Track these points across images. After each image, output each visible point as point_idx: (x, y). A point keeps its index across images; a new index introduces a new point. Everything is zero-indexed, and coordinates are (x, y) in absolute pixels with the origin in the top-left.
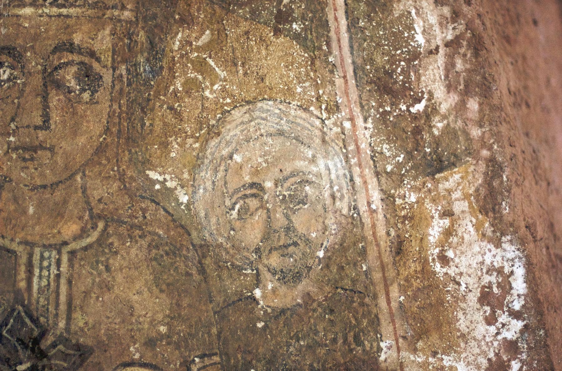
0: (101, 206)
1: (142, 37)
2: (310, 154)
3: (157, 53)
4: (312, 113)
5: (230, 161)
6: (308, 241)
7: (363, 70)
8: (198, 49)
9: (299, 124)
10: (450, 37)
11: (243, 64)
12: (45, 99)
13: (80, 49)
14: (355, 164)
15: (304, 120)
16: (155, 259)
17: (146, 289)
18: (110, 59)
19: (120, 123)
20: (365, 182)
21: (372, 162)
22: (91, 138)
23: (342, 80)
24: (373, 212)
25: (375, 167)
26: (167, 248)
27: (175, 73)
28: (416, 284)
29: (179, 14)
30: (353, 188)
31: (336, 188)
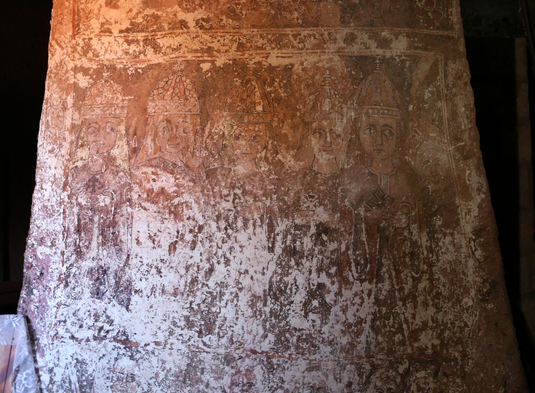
1: (402, 124)
2: (440, 154)
6: (439, 174)
8: (415, 127)
12: (382, 138)
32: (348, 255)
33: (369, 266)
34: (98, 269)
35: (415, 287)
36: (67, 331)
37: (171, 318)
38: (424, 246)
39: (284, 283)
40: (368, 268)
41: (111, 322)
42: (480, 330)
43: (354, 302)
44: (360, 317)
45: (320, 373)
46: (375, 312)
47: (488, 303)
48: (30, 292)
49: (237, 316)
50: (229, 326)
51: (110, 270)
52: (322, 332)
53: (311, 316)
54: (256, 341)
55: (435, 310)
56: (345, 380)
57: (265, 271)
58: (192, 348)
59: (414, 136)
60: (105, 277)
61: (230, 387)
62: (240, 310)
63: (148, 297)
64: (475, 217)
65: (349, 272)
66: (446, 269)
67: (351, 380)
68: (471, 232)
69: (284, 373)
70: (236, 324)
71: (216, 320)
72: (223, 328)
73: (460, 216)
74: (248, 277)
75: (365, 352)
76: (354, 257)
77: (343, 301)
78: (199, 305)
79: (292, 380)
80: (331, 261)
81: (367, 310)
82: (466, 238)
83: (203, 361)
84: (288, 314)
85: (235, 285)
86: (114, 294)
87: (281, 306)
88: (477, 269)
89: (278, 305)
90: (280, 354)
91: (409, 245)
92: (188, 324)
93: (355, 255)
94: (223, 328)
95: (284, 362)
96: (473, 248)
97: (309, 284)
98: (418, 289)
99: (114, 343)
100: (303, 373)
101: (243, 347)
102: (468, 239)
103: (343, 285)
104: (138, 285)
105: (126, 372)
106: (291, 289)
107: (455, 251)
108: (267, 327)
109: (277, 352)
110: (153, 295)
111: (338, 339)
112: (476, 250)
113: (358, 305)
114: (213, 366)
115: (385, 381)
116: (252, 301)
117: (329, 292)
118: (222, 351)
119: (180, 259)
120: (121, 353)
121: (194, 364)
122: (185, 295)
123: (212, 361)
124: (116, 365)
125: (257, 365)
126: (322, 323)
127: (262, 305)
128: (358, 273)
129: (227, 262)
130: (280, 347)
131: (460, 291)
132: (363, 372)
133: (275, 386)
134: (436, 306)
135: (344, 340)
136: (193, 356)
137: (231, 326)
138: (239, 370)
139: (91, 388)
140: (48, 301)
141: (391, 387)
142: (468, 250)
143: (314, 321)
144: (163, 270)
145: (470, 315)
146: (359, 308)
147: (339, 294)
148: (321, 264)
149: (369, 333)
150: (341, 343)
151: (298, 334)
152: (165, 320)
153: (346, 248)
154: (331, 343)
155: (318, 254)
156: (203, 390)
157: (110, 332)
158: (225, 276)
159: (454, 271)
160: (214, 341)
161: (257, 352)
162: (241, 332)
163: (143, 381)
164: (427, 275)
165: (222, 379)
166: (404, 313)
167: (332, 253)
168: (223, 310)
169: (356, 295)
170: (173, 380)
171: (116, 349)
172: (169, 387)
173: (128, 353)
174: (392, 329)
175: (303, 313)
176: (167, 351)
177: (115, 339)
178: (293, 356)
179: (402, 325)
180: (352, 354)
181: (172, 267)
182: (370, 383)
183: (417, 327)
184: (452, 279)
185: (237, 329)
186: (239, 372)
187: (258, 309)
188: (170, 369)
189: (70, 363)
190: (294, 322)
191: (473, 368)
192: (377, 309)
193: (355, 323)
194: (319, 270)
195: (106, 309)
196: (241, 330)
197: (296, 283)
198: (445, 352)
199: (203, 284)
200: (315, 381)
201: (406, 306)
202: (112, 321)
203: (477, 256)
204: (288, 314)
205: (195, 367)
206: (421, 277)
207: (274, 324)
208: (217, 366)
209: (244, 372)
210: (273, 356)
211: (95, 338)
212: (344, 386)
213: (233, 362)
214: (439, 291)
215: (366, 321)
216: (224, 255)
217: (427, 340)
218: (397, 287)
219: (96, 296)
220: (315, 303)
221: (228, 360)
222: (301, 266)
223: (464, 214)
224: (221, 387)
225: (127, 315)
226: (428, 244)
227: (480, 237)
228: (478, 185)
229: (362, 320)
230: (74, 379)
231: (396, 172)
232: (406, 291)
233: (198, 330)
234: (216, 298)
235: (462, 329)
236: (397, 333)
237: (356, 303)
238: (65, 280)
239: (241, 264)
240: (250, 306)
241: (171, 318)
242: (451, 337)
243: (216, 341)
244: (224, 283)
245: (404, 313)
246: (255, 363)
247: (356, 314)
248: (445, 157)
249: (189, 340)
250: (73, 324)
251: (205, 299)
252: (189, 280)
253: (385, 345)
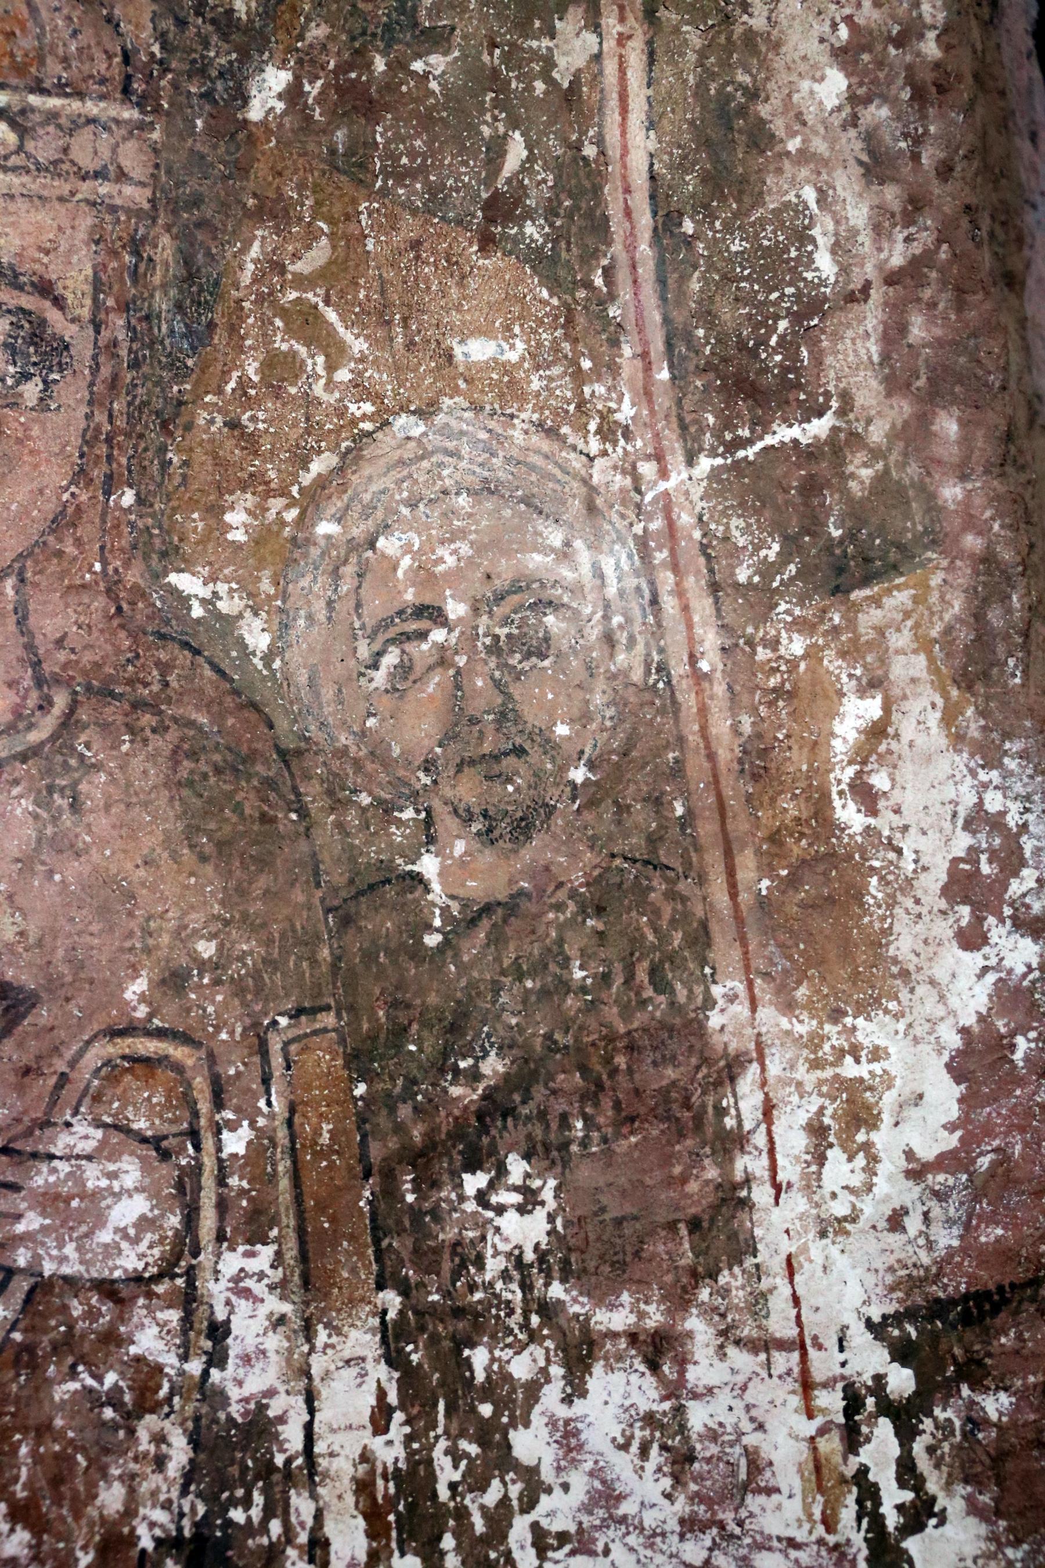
0: (62, 656)
1: (165, 249)
2: (556, 538)
3: (201, 291)
4: (562, 439)
5: (369, 553)
6: (550, 745)
7: (688, 337)
8: (301, 282)
9: (533, 468)
10: (897, 260)
11: (405, 320)
13: (16, 276)
14: (663, 563)
15: (547, 457)
16: (190, 784)
17: (165, 855)
18: (88, 302)
19: (110, 458)
20: (686, 609)
21: (702, 560)
22: (41, 492)
23: (639, 363)
24: (699, 678)
25: (711, 571)
26: (217, 757)
27: (243, 338)
28: (798, 848)
29: (255, 195)
30: (659, 624)
31: (617, 620)
38: (341, 1466)
59: (280, 369)
64: (917, 1171)
73: (749, 1163)
82: (807, 1385)
96: (893, 1497)
102: (832, 1401)
107: (689, 1526)
112: (920, 1514)
142: (830, 1523)
223: (792, 1142)
226: (390, 1451)
227: (975, 1373)
228: (962, 842)
231: (68, 722)
248: (617, 563)
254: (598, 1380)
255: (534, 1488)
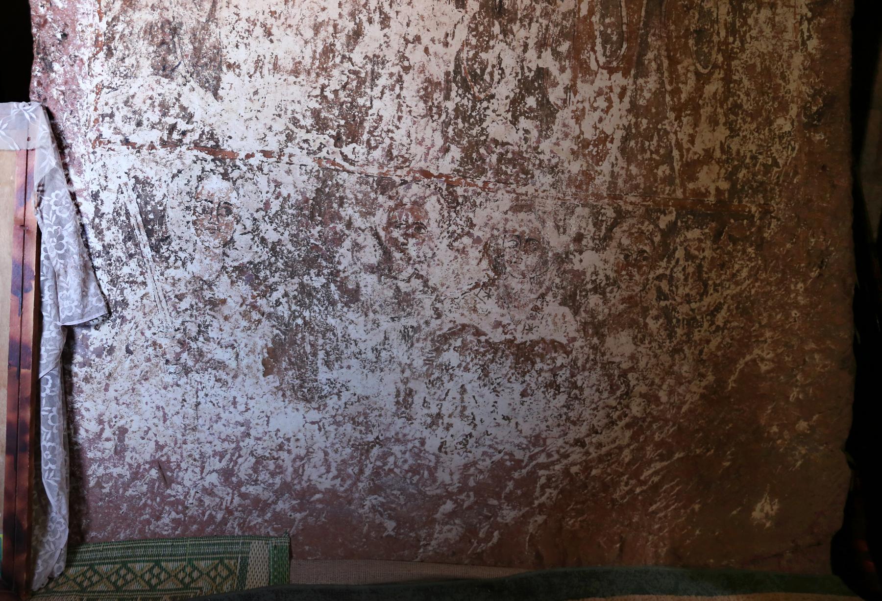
32: (591, 23)
33: (625, 46)
34: (162, 26)
35: (699, 89)
36: (117, 131)
37: (289, 112)
38: (722, 21)
39: (481, 63)
40: (623, 50)
41: (189, 118)
42: (796, 173)
43: (595, 105)
44: (603, 132)
45: (532, 216)
46: (630, 125)
47: (816, 131)
48: (48, 68)
49: (400, 114)
50: (386, 129)
51: (184, 28)
52: (539, 150)
53: (524, 123)
54: (430, 157)
55: (728, 132)
56: (573, 230)
57: (449, 39)
58: (324, 163)
60: (176, 39)
61: (385, 229)
62: (404, 105)
63: (250, 77)
65: (591, 53)
66: (754, 65)
67: (582, 231)
68: (807, 5)
69: (474, 211)
70: (398, 128)
71: (364, 120)
72: (375, 134)
74: (420, 48)
75: (608, 188)
76: (602, 28)
77: (578, 102)
78: (336, 92)
79: (487, 224)
80: (561, 31)
81: (616, 121)
82: (795, 14)
83: (342, 185)
84: (485, 116)
85: (397, 62)
86: (191, 69)
87: (474, 102)
88: (807, 72)
89: (469, 99)
90: (469, 180)
91: (697, 16)
92: (317, 124)
93: (603, 24)
94: (375, 134)
95: (474, 194)
96: (806, 34)
97: (522, 68)
98: (703, 93)
99: (195, 152)
100: (506, 213)
101: (408, 166)
102: (798, 17)
103: (580, 75)
104: (232, 55)
105: (216, 200)
106: (491, 74)
107: (774, 37)
108: (450, 136)
109: (465, 178)
110: (258, 74)
111: (566, 164)
112: (810, 37)
113: (602, 110)
114: (358, 194)
115: (636, 238)
116: (426, 89)
117: (555, 84)
118: (373, 170)
119: (303, 12)
120: (208, 168)
121: (327, 190)
122: (313, 75)
123: (358, 186)
124: (200, 188)
125: (430, 195)
126: (540, 135)
127: (442, 96)
128: (607, 57)
129: (385, 21)
130: (470, 169)
131: (772, 106)
132: (602, 221)
133: (459, 231)
134: (730, 125)
135: (575, 167)
136: (326, 175)
137: (389, 131)
138: (401, 201)
139: (161, 224)
140: (80, 81)
141: (645, 248)
143: (527, 131)
144: (274, 31)
145: (784, 148)
146: (604, 116)
147: (571, 89)
148: (545, 35)
149: (617, 159)
150: (569, 171)
151: (499, 150)
152: (279, 116)
153: (589, 11)
154: (553, 170)
155: (541, 16)
156: (342, 231)
157: (189, 134)
158: (381, 45)
159: (767, 73)
160: (360, 155)
161: (432, 175)
162: (405, 141)
163: (245, 215)
164: (722, 72)
165: (374, 215)
166: (676, 133)
167: (565, 16)
168: (377, 103)
169: (599, 93)
170: (293, 215)
171: (199, 162)
172: (288, 225)
173: (218, 169)
174: (654, 156)
175: (509, 116)
176: (283, 166)
177: (197, 145)
178: (491, 186)
179: (671, 152)
180: (587, 190)
181: (290, 26)
182: (611, 238)
183: (696, 157)
184: (762, 84)
185: (399, 136)
186: (400, 205)
187: (436, 103)
188: (289, 195)
189: (126, 184)
190: (494, 129)
191: (775, 234)
192: (634, 120)
193: (595, 141)
194: (541, 45)
195: (180, 95)
196: (405, 138)
197: (500, 64)
198: (736, 203)
199: (344, 57)
200: (524, 228)
201: (681, 121)
202: (191, 116)
203: (810, 48)
204: (485, 116)
205: (329, 195)
206: (711, 74)
207: (461, 130)
208: (366, 194)
209: (409, 206)
210: (458, 183)
211: (164, 144)
212: (569, 239)
213: (392, 189)
214: (739, 101)
215: (613, 139)
216: (380, 8)
217: (709, 180)
218: (669, 88)
219: (161, 72)
220: (531, 101)
221: (384, 185)
222: (511, 36)
224: (371, 227)
225: (216, 106)
226: (730, 20)
227: (821, 15)
229: (607, 136)
230: (133, 209)
232: (684, 96)
233: (334, 133)
234: (365, 82)
235: (767, 169)
236: (663, 164)
237: (598, 107)
238: (105, 45)
239: (408, 25)
240: (421, 97)
241: (289, 112)
242: (748, 179)
243: (364, 154)
244: (378, 57)
245: (676, 133)
246: (428, 192)
247: (598, 125)
249: (320, 149)
250: (126, 119)
251: (347, 83)
252: (320, 50)
253: (640, 180)
254: (763, 11)
255: (750, 29)
